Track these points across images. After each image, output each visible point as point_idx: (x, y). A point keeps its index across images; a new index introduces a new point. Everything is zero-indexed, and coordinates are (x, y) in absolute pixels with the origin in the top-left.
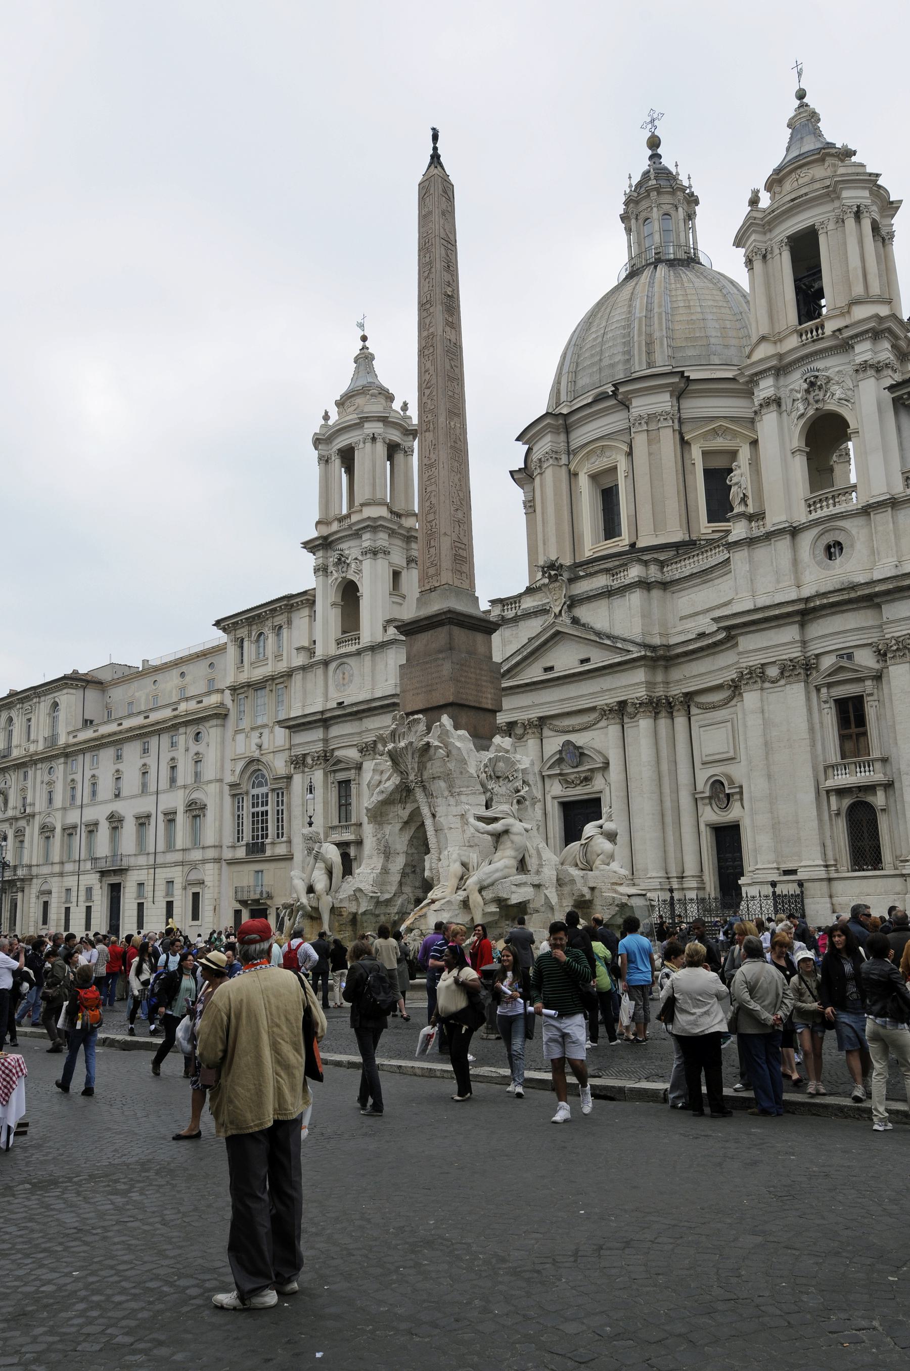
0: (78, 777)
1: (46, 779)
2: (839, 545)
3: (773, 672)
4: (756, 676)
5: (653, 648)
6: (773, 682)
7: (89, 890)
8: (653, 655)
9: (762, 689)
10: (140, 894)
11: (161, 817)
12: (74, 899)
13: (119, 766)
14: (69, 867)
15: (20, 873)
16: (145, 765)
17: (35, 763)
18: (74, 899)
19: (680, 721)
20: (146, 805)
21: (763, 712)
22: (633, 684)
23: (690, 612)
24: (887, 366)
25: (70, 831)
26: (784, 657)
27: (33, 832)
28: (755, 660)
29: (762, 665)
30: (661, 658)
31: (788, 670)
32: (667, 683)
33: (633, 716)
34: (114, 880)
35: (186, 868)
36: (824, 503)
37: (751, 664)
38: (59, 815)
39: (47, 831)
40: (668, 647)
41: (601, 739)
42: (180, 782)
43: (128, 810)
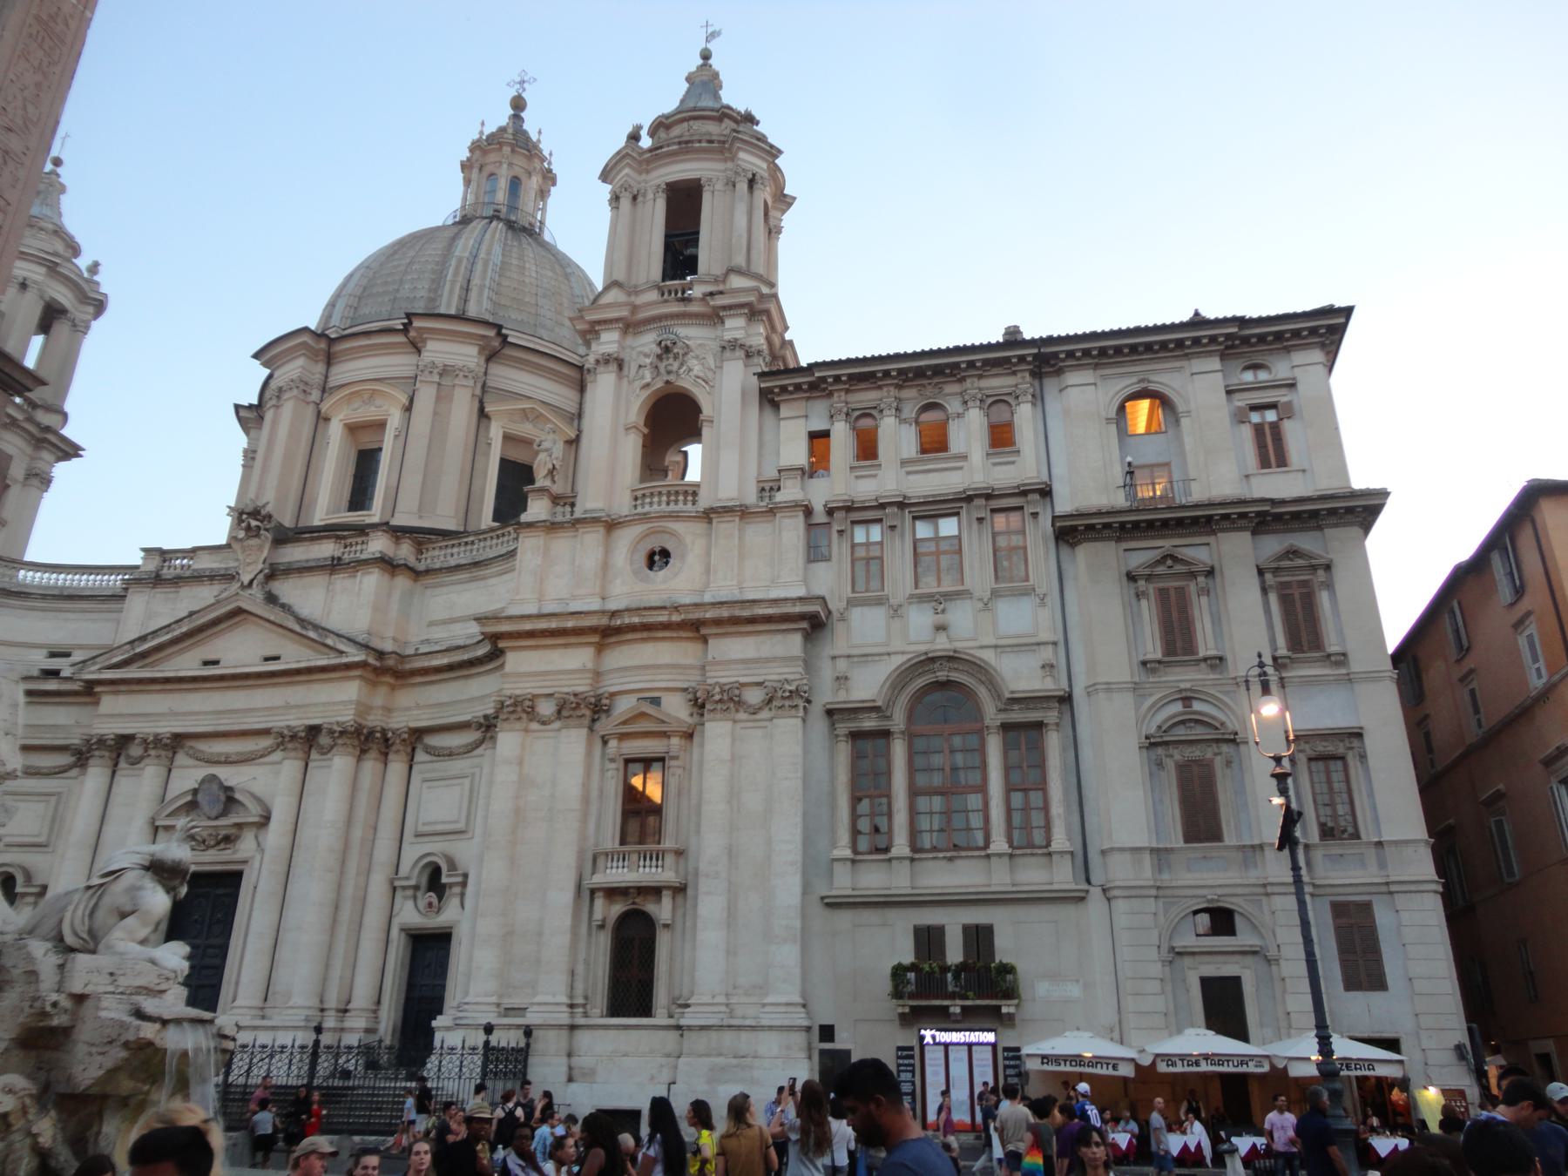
2: (665, 554)
3: (546, 708)
4: (521, 709)
5: (381, 654)
6: (544, 723)
8: (378, 664)
9: (526, 730)
19: (397, 767)
21: (521, 763)
22: (337, 701)
23: (449, 613)
24: (759, 352)
26: (566, 690)
28: (523, 688)
29: (535, 696)
30: (387, 668)
31: (567, 709)
32: (388, 710)
33: (325, 751)
36: (656, 499)
37: (518, 692)
40: (403, 658)
41: (267, 781)
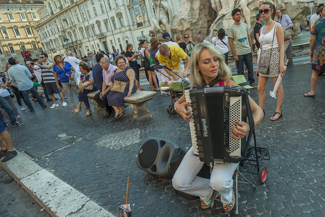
0: (84, 12)
1: (75, 14)
7: (98, 44)
10: (112, 43)
11: (110, 20)
12: (95, 47)
13: (94, 6)
14: (90, 39)
15: (78, 42)
16: (101, 4)
17: (70, 9)
18: (95, 47)
20: (105, 17)
25: (87, 28)
27: (78, 31)
34: (104, 40)
35: (122, 34)
38: (82, 24)
39: (81, 28)
42: (112, 8)
43: (101, 18)
